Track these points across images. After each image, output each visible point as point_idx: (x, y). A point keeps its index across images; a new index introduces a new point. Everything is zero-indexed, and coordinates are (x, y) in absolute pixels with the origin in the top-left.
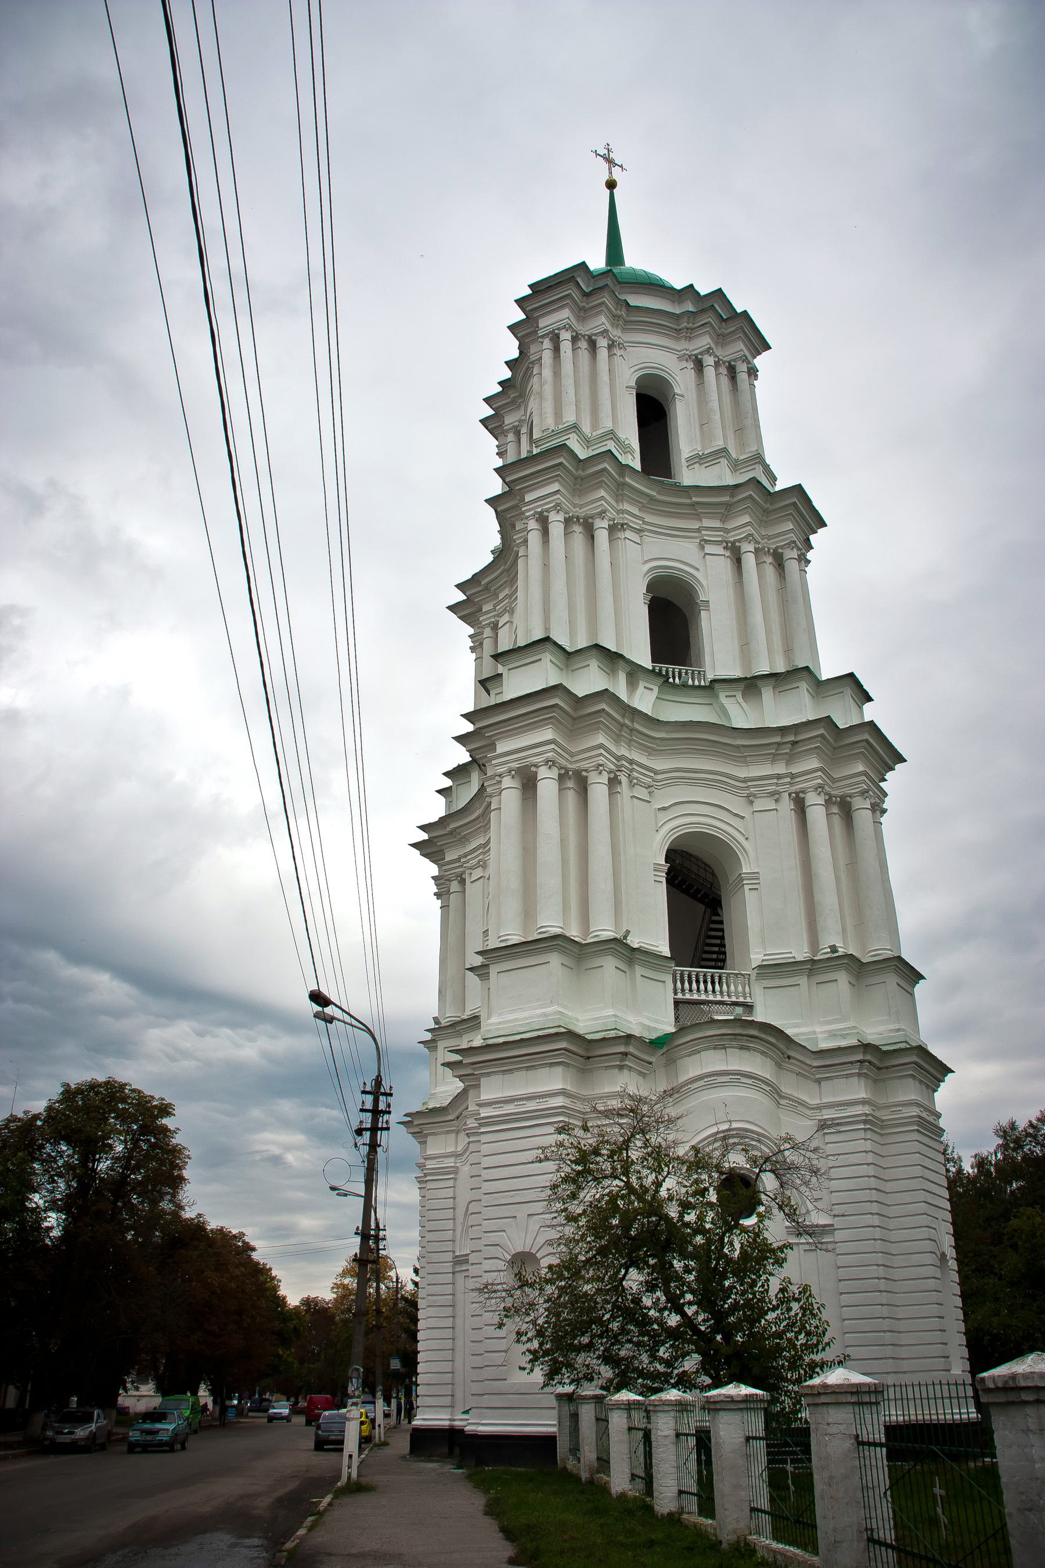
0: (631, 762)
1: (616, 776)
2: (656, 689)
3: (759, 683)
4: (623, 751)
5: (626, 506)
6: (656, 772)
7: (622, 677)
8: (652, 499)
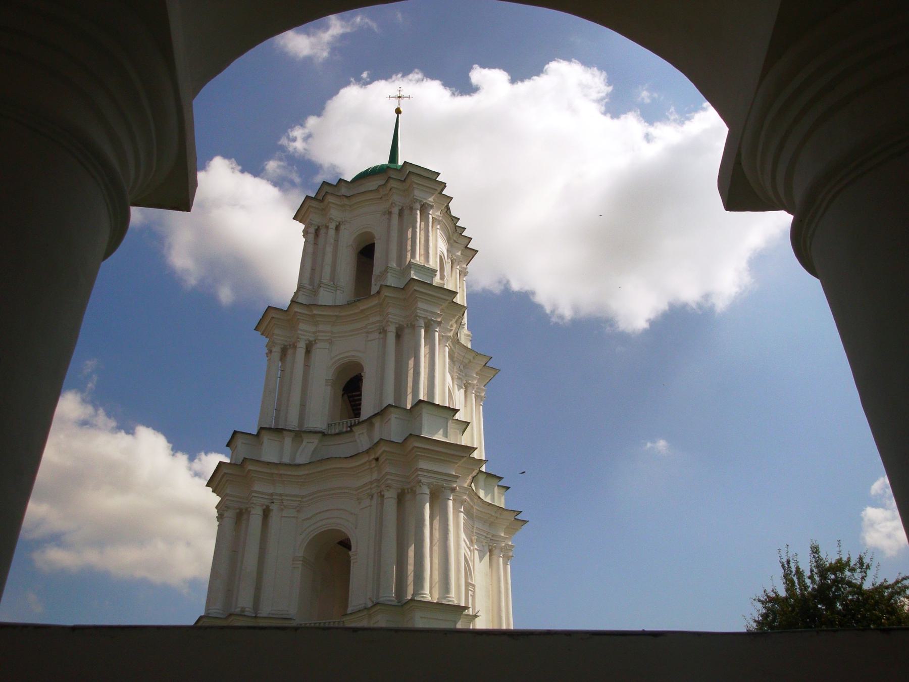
0: (281, 495)
1: (268, 507)
2: (316, 441)
3: (373, 420)
4: (279, 490)
5: (322, 327)
6: (303, 497)
7: (288, 440)
8: (336, 316)
